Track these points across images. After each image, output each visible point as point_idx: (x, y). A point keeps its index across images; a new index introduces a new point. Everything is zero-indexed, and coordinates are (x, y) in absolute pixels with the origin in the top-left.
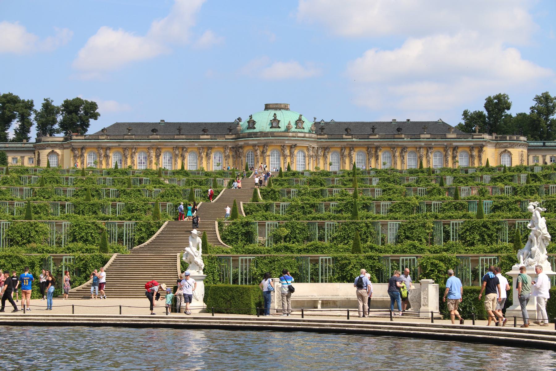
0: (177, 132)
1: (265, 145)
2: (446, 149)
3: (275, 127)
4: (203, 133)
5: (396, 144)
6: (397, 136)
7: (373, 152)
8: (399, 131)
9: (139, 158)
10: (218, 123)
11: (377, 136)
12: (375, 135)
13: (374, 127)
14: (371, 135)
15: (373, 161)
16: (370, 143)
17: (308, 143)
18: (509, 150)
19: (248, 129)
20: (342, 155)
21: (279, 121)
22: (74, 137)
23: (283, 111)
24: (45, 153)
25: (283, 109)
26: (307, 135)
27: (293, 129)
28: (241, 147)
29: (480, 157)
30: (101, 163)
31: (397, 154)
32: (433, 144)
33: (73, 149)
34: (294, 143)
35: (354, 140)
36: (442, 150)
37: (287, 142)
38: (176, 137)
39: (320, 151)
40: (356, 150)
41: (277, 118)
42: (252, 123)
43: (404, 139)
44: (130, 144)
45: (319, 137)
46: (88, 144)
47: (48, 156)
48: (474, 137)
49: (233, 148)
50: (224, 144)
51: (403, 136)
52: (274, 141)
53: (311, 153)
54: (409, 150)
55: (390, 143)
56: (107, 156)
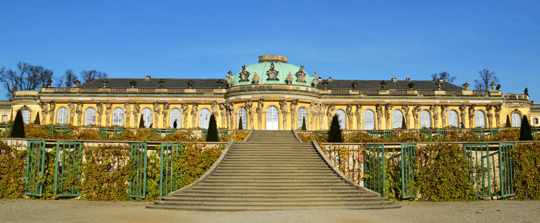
2: (461, 107)
3: (273, 79)
5: (409, 101)
6: (409, 92)
8: (411, 87)
9: (115, 114)
10: (207, 80)
11: (388, 92)
15: (383, 119)
17: (311, 98)
19: (240, 81)
23: (280, 63)
25: (279, 61)
26: (310, 89)
27: (294, 82)
29: (497, 116)
30: (72, 119)
31: (410, 112)
33: (42, 104)
35: (361, 96)
38: (157, 90)
43: (417, 95)
44: (104, 99)
45: (322, 92)
46: (58, 98)
48: (491, 94)
49: (223, 104)
50: (212, 99)
51: (416, 92)
52: (272, 96)
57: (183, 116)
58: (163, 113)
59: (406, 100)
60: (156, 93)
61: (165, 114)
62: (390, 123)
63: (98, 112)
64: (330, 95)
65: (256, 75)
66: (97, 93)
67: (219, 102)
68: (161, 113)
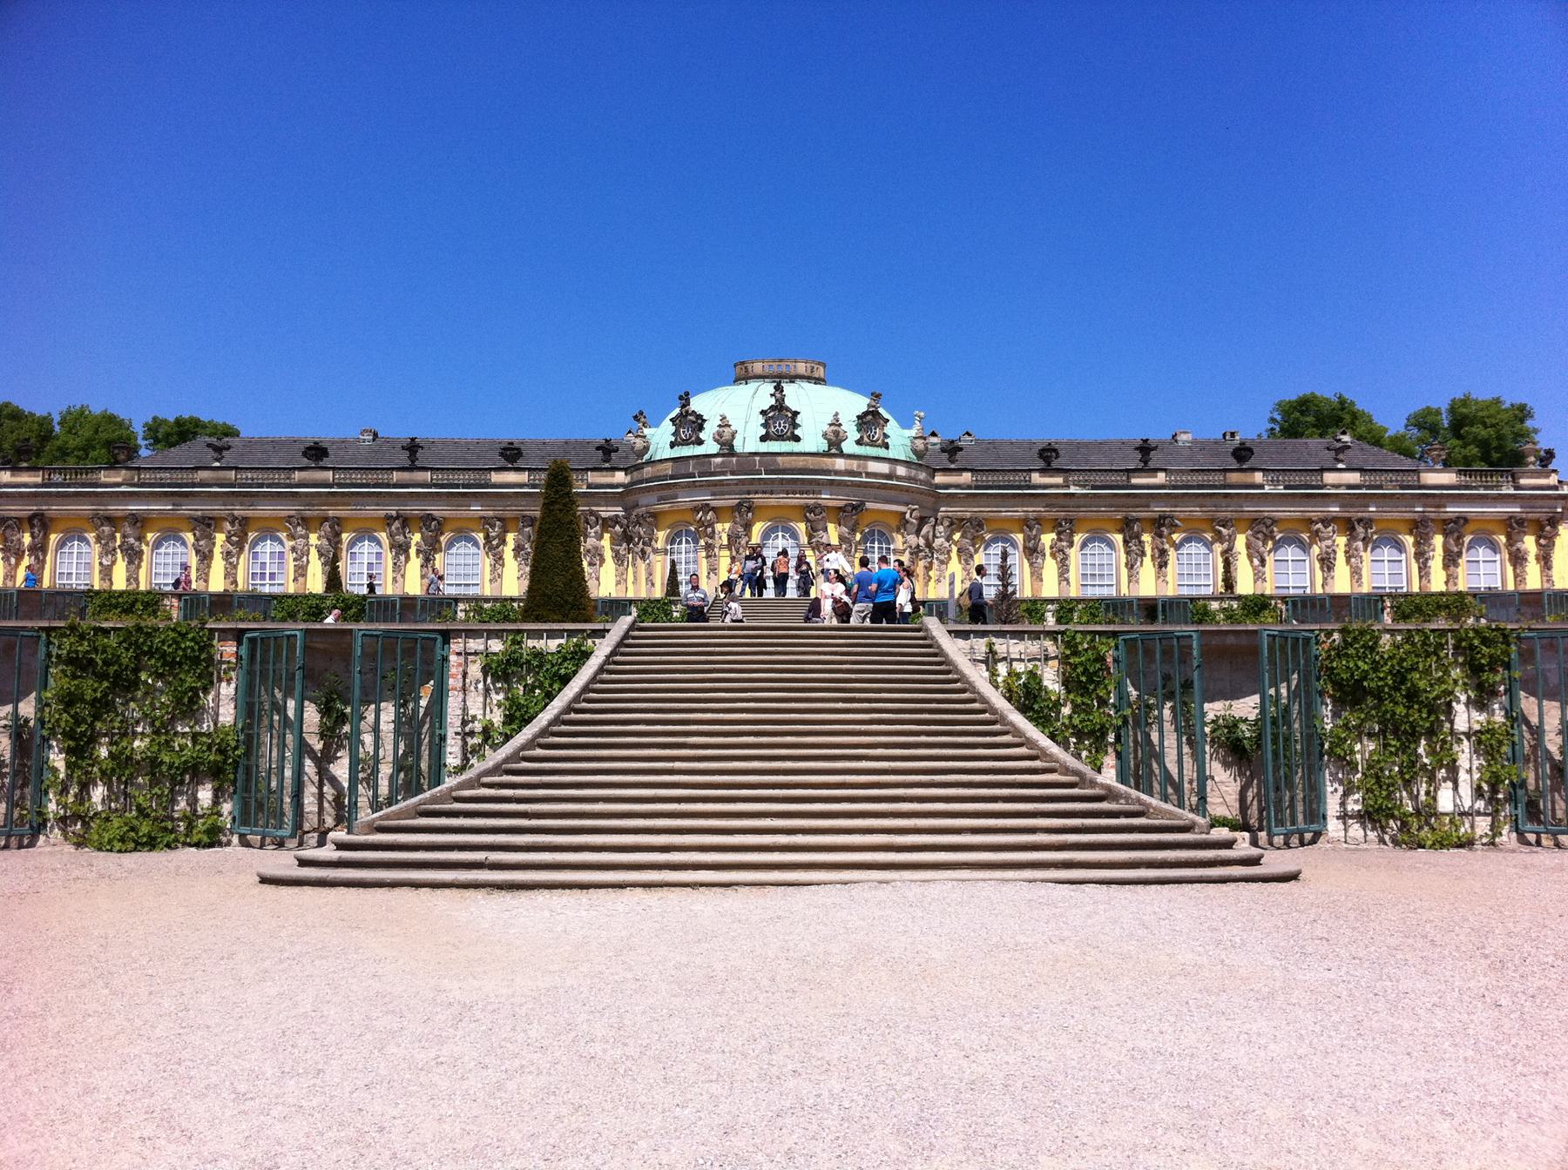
0: (403, 458)
3: (780, 437)
4: (502, 463)
6: (1234, 477)
11: (1161, 478)
12: (1156, 470)
15: (1147, 568)
19: (672, 445)
21: (796, 414)
23: (805, 385)
25: (802, 377)
26: (901, 471)
27: (849, 447)
30: (107, 572)
35: (1073, 490)
38: (396, 476)
43: (1261, 487)
49: (615, 520)
51: (1258, 477)
57: (488, 561)
58: (418, 552)
60: (395, 486)
62: (1169, 578)
63: (197, 552)
64: (969, 487)
65: (724, 423)
66: (194, 485)
67: (603, 515)
68: (413, 551)
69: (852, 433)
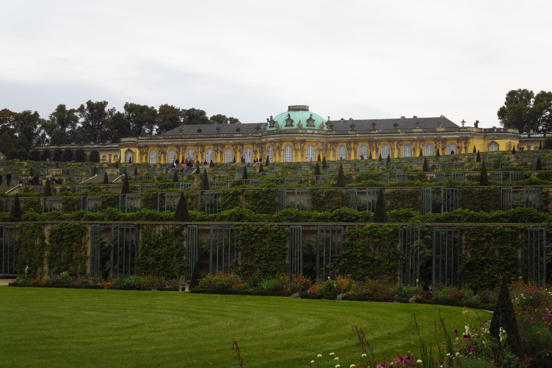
1: (280, 141)
2: (436, 140)
3: (289, 126)
5: (393, 137)
6: (393, 131)
7: (374, 145)
11: (377, 131)
12: (375, 130)
13: (374, 124)
14: (371, 130)
16: (370, 138)
18: (496, 141)
20: (349, 149)
22: (140, 138)
23: (301, 112)
24: (123, 150)
28: (265, 143)
29: (466, 148)
30: (160, 158)
31: (395, 147)
32: (424, 137)
33: (139, 147)
34: (303, 138)
36: (433, 143)
37: (297, 138)
39: (329, 145)
40: (360, 144)
41: (292, 118)
42: (272, 122)
44: (181, 143)
46: (150, 143)
47: (125, 153)
49: (259, 144)
50: (252, 141)
52: (287, 138)
53: (320, 147)
54: (405, 143)
55: (387, 138)
56: (164, 153)
59: (390, 137)
61: (222, 153)
63: (177, 152)
69: (304, 124)
